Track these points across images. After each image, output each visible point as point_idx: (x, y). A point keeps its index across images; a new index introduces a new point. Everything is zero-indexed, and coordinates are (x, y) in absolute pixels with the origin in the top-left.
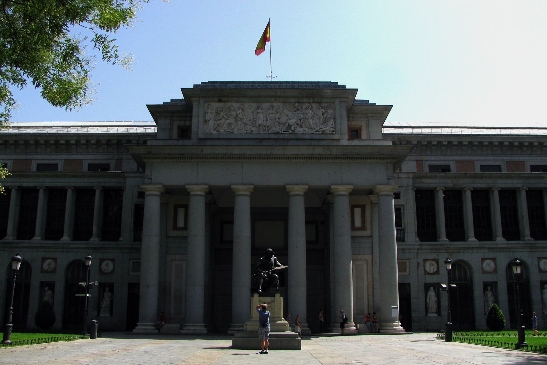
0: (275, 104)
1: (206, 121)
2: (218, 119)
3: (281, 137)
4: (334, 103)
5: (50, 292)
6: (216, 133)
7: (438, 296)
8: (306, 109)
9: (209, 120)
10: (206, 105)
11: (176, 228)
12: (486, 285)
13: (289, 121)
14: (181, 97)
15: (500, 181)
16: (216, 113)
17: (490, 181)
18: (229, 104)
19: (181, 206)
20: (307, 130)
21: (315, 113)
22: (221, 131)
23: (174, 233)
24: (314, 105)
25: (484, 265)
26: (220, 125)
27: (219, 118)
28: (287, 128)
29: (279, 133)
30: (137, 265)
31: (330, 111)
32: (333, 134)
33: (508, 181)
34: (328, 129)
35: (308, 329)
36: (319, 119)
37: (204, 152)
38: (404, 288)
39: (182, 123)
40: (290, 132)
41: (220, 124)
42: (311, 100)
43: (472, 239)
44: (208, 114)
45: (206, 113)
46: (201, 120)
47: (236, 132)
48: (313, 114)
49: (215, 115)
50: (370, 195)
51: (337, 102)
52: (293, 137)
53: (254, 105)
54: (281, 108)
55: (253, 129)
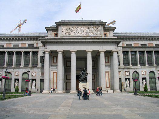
3: (84, 36)
5: (17, 81)
7: (129, 81)
8: (92, 28)
11: (54, 63)
12: (143, 78)
15: (147, 49)
17: (144, 49)
18: (69, 27)
19: (55, 56)
20: (92, 34)
23: (53, 64)
24: (94, 27)
25: (143, 73)
30: (43, 73)
33: (149, 49)
34: (98, 33)
36: (96, 31)
38: (120, 79)
39: (55, 32)
43: (139, 65)
46: (61, 31)
52: (88, 36)
53: (77, 27)
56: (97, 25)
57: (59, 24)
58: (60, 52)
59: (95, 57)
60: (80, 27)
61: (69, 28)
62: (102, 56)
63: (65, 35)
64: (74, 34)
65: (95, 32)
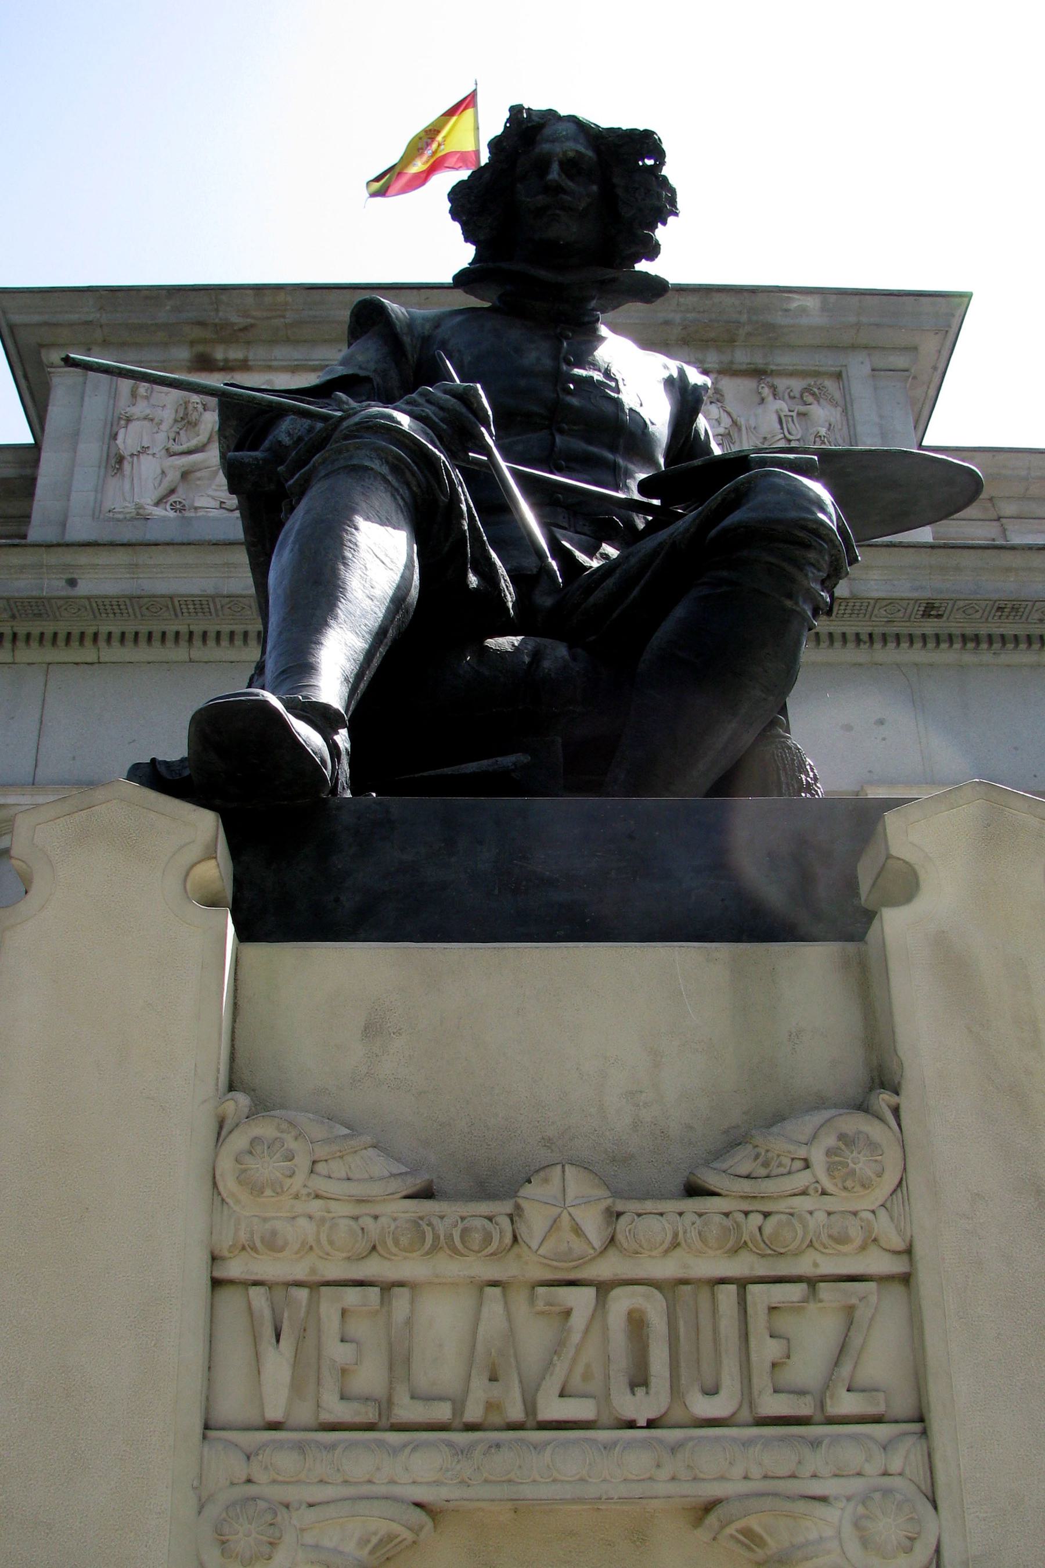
1: (116, 462)
2: (184, 447)
4: (838, 376)
6: (172, 514)
9: (132, 455)
16: (176, 421)
21: (742, 421)
22: (197, 504)
26: (198, 474)
27: (194, 443)
37: (84, 588)
41: (200, 470)
44: (134, 426)
45: (123, 422)
46: (90, 450)
48: (726, 421)
49: (175, 429)
51: (858, 367)
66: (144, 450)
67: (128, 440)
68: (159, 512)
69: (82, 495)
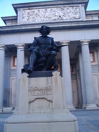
0: (53, 8)
3: (56, 21)
8: (67, 9)
10: (24, 11)
13: (60, 14)
14: (15, 14)
18: (33, 10)
20: (67, 17)
24: (70, 8)
28: (59, 17)
29: (55, 20)
31: (77, 10)
32: (80, 18)
34: (77, 16)
35: (74, 107)
40: (61, 19)
42: (69, 5)
46: (21, 17)
47: (37, 21)
50: (96, 47)
52: (62, 21)
54: (56, 10)
55: (44, 19)
56: (74, 5)
57: (16, 7)
58: (20, 46)
59: (74, 58)
60: (49, 10)
61: (34, 12)
62: (86, 49)
63: (27, 23)
64: (40, 20)
65: (72, 15)
66: (25, 16)
67: (24, 16)
68: (27, 21)
69: (21, 21)
